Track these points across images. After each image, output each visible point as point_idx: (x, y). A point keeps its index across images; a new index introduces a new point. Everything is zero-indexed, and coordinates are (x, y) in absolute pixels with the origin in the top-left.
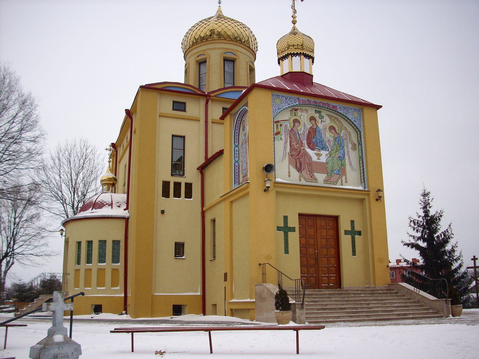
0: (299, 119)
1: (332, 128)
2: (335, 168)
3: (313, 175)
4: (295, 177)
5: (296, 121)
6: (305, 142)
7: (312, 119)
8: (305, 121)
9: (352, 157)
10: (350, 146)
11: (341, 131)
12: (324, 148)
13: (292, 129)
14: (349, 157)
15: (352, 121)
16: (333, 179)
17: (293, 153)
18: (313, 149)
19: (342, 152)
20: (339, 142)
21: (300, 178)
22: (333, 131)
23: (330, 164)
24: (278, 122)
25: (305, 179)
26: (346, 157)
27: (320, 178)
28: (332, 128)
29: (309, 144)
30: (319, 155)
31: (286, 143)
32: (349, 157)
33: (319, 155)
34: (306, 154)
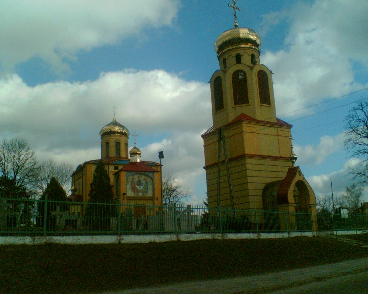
1: (144, 179)
4: (133, 195)
5: (133, 178)
6: (136, 184)
7: (138, 177)
9: (150, 187)
10: (150, 184)
12: (142, 185)
13: (132, 181)
14: (149, 187)
17: (132, 188)
20: (147, 183)
26: (149, 187)
28: (144, 179)
31: (130, 185)
32: (149, 187)
34: (136, 188)
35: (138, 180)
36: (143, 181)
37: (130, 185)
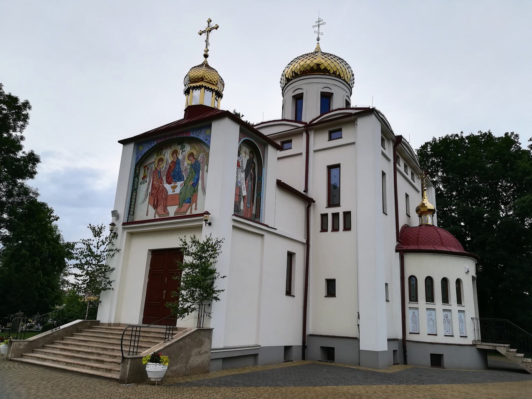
0: (163, 157)
2: (187, 197)
3: (167, 209)
6: (164, 178)
8: (168, 157)
11: (199, 155)
12: (180, 179)
15: (204, 140)
16: (183, 209)
18: (170, 183)
19: (197, 176)
21: (155, 214)
22: (192, 158)
23: (183, 194)
24: (146, 166)
25: (159, 215)
26: (200, 182)
27: (172, 210)
28: (191, 155)
29: (167, 178)
30: (174, 188)
31: (149, 184)
33: (174, 188)
35: (172, 162)
36: (186, 163)
37: (149, 184)
